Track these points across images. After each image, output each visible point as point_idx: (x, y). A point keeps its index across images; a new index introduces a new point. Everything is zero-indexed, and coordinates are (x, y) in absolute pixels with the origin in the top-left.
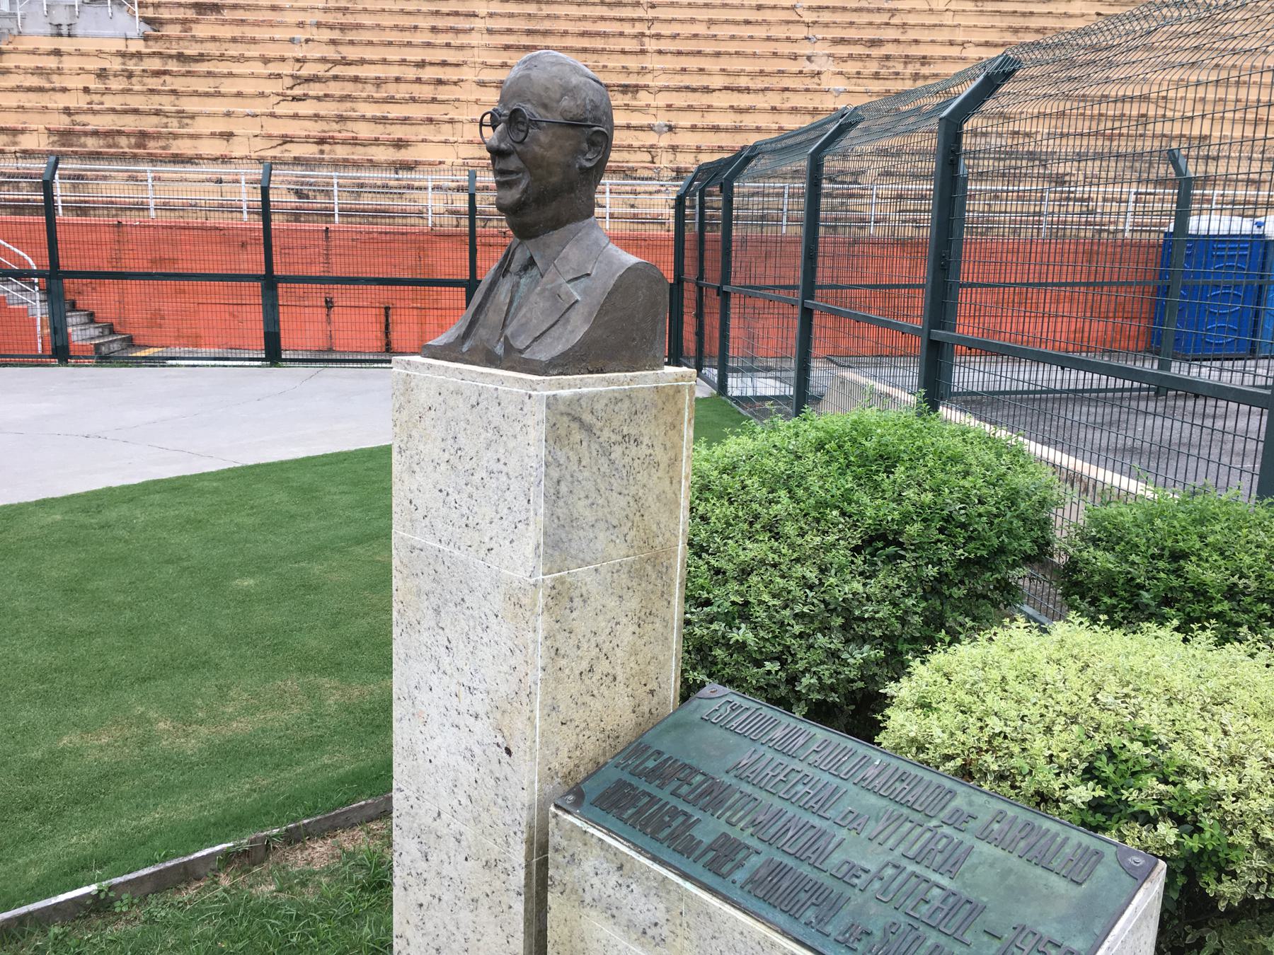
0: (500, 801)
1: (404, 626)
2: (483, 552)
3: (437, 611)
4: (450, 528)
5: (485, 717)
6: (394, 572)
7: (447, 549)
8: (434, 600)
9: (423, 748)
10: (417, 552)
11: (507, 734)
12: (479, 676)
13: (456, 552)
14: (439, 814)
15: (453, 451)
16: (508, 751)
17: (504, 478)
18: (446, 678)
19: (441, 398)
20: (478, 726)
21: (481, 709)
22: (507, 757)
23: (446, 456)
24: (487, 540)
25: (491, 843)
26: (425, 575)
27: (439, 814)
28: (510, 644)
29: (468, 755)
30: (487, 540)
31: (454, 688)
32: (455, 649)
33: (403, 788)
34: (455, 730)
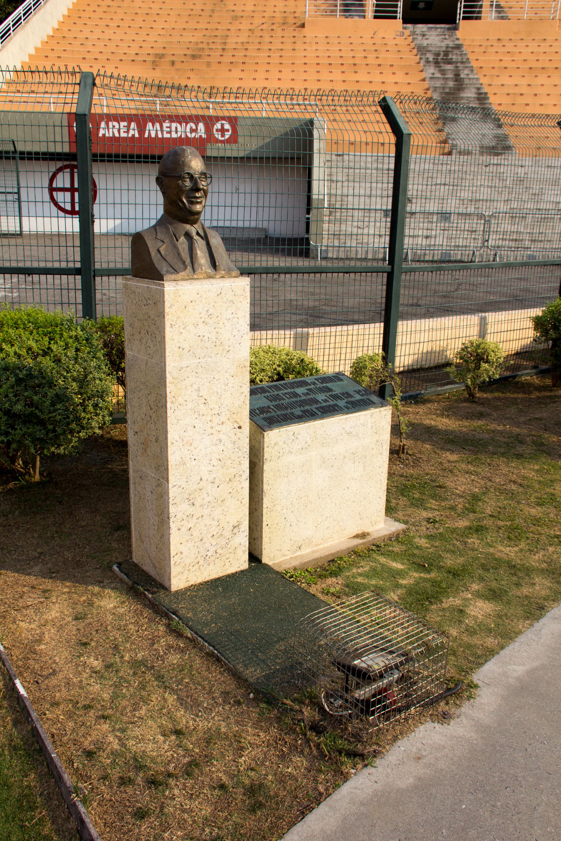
0: (236, 450)
1: (176, 408)
2: (224, 354)
3: (198, 390)
4: (205, 351)
5: (227, 421)
6: (168, 384)
7: (204, 360)
8: (196, 387)
9: (189, 457)
10: (185, 369)
11: (238, 421)
12: (224, 405)
13: (209, 359)
14: (201, 479)
15: (206, 317)
16: (240, 427)
17: (236, 319)
18: (204, 417)
19: (199, 296)
20: (223, 428)
21: (223, 419)
22: (240, 430)
23: (202, 320)
24: (227, 347)
25: (232, 470)
26: (190, 377)
27: (201, 479)
28: (240, 384)
29: (218, 442)
30: (227, 347)
31: (209, 418)
32: (209, 402)
33: (175, 484)
34: (211, 436)
